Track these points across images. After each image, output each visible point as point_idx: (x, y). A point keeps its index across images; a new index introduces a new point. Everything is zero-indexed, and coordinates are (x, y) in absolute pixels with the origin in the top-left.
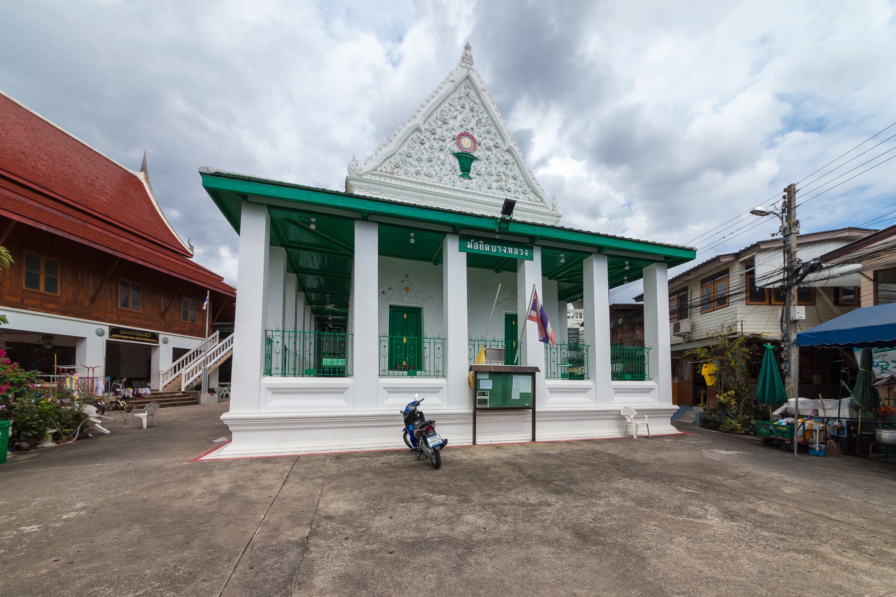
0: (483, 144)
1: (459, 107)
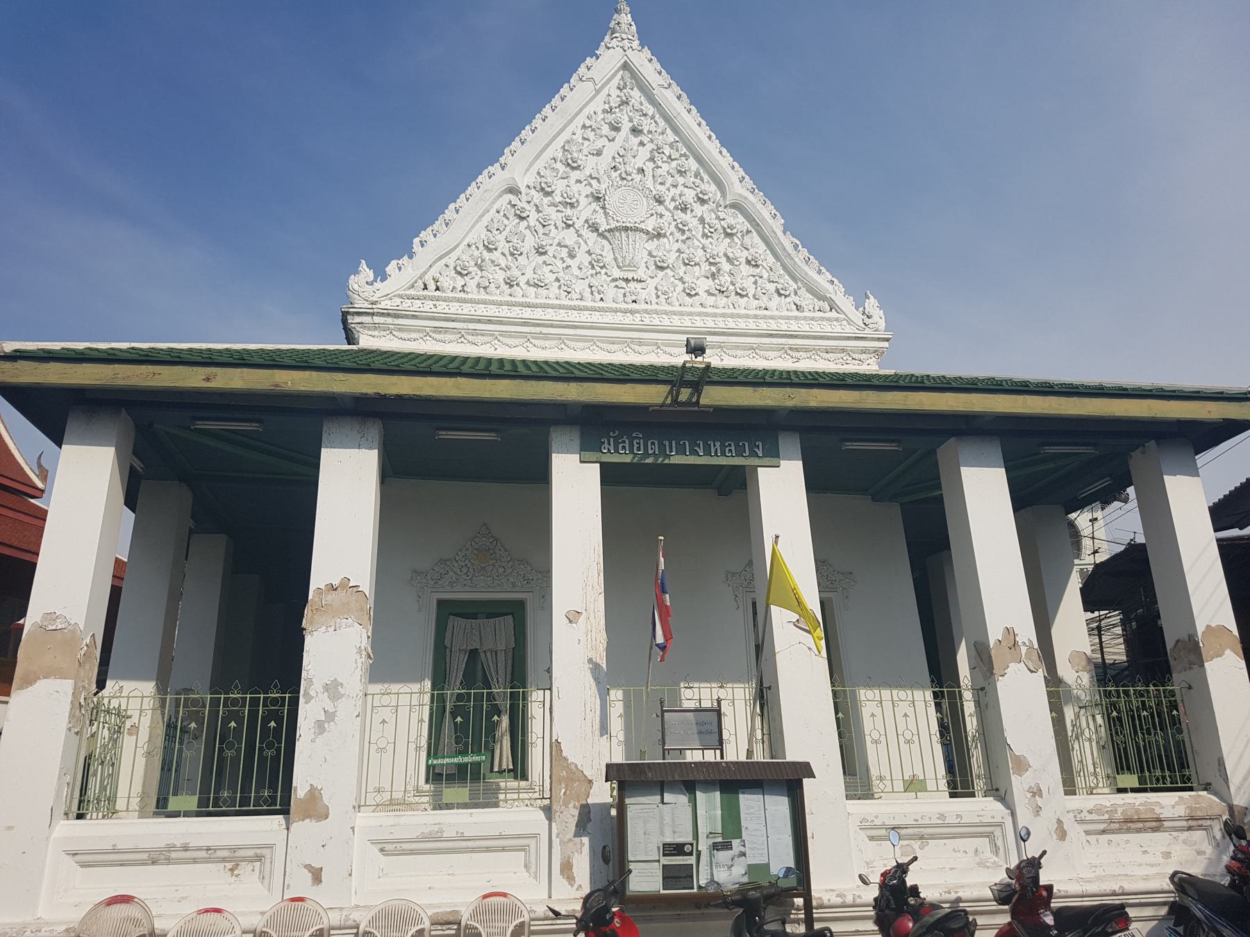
1: (606, 130)
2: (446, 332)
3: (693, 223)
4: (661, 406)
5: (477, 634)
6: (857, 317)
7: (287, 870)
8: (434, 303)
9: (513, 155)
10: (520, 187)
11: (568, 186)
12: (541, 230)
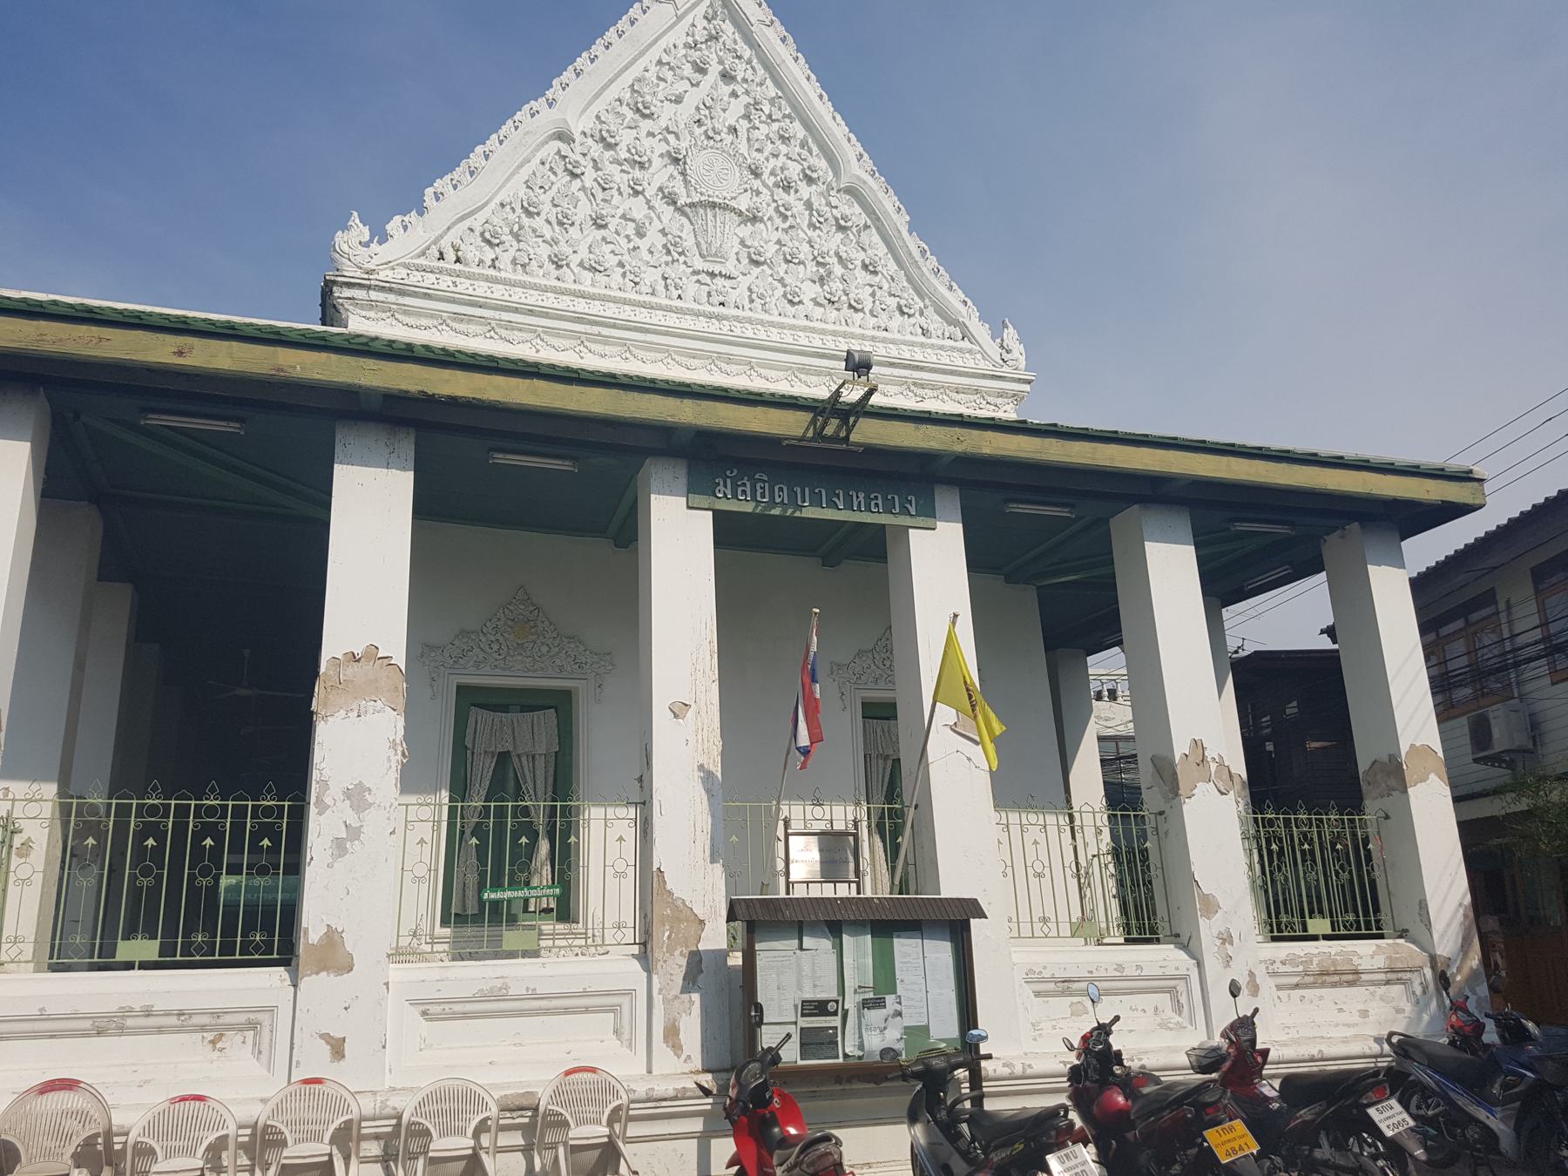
1: (688, 70)
2: (469, 322)
3: (799, 207)
4: (802, 439)
5: (510, 731)
6: (993, 349)
7: (295, 1041)
8: (454, 279)
9: (564, 89)
11: (637, 138)
12: (600, 195)
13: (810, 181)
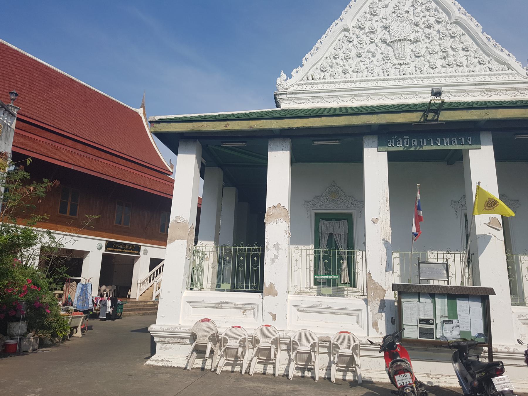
0: (421, 24)
8: (311, 86)
9: (346, 14)
10: (349, 27)
12: (359, 46)
13: (439, 22)
